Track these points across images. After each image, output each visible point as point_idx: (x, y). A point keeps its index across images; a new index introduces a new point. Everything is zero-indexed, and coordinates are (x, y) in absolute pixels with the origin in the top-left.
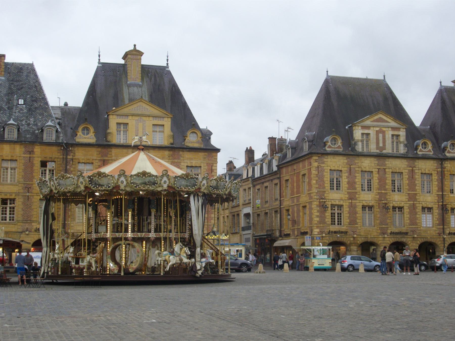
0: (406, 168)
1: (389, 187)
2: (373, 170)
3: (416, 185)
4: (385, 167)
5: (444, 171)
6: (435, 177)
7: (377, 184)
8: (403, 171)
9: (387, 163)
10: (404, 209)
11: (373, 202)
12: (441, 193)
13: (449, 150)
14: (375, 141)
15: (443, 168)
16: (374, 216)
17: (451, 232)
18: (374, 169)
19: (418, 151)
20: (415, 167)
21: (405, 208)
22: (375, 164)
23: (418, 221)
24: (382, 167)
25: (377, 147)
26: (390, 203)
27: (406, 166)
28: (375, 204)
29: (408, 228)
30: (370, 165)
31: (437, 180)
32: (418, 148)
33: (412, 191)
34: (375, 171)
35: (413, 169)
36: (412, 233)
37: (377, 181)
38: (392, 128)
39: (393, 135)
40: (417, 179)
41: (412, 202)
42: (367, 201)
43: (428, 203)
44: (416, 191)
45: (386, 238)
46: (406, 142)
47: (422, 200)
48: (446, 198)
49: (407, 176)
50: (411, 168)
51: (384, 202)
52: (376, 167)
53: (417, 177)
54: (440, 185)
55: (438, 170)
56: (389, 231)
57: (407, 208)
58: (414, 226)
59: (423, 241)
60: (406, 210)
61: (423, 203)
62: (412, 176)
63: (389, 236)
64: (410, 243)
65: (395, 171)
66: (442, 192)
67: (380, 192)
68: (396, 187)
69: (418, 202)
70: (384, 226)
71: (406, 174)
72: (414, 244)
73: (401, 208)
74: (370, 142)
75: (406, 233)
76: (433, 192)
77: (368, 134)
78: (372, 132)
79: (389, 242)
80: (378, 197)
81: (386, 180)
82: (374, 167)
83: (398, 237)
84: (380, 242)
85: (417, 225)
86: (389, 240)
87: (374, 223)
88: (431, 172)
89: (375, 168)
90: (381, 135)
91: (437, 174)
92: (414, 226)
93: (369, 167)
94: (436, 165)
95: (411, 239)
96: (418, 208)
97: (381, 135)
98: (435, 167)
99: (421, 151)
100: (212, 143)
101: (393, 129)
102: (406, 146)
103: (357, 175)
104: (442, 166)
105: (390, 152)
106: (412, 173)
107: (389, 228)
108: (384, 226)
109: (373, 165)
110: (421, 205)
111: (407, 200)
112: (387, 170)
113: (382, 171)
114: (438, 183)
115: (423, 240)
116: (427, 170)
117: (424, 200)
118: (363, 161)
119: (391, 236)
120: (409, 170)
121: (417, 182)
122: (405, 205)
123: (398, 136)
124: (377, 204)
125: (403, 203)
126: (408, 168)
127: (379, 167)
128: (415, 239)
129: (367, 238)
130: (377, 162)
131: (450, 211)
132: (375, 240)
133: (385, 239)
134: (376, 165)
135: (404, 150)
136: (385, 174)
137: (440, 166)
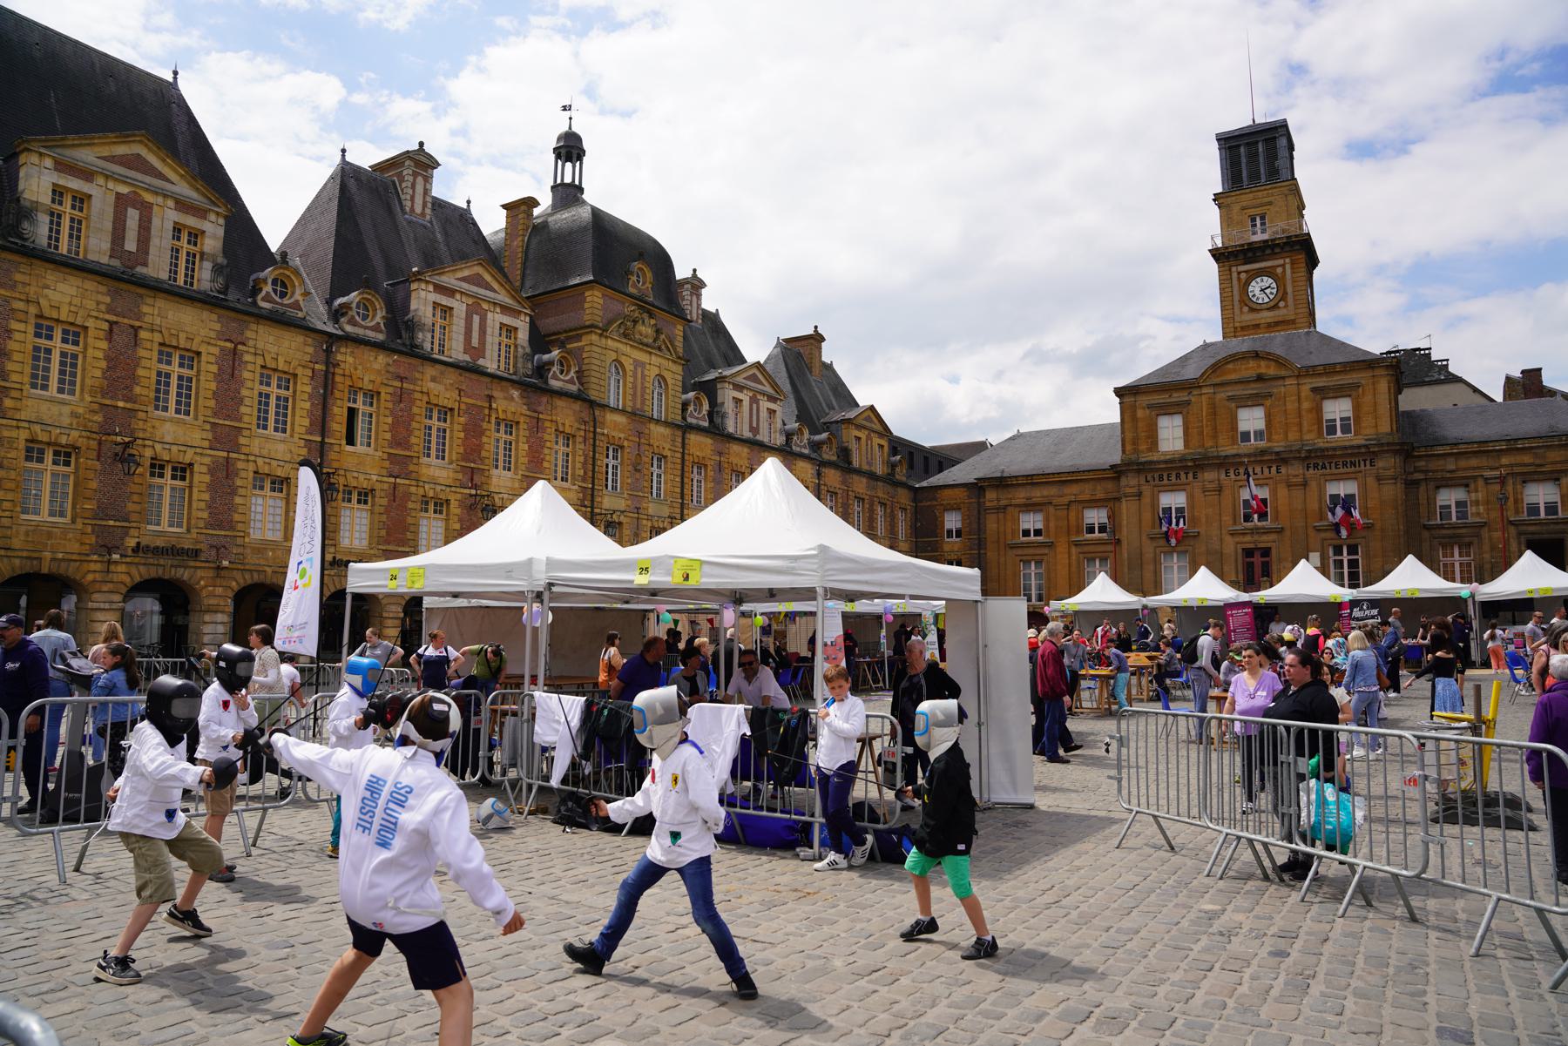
0: (212, 341)
1: (145, 392)
2: (90, 323)
3: (241, 401)
4: (137, 324)
5: (334, 374)
6: (305, 387)
7: (98, 373)
8: (203, 349)
9: (145, 309)
10: (192, 473)
11: (75, 434)
12: (319, 439)
13: (353, 317)
14: (109, 226)
15: (330, 364)
16: (76, 485)
17: (338, 557)
18: (91, 320)
19: (260, 297)
20: (244, 344)
21: (196, 468)
22: (98, 303)
23: (237, 517)
24: (126, 321)
25: (112, 249)
26: (144, 446)
27: (213, 334)
28: (82, 442)
29: (202, 538)
30: (76, 301)
31: (311, 396)
32: (261, 290)
33: (227, 417)
34: (96, 327)
35: (235, 348)
36: (213, 552)
37: (103, 364)
38: (177, 202)
39: (177, 230)
40: (249, 384)
41: (225, 454)
42: (49, 428)
43: (274, 463)
44: (240, 420)
45: (116, 562)
46: (221, 260)
47: (256, 451)
48: (332, 456)
49: (214, 368)
50: (228, 345)
51: (119, 439)
52: (101, 316)
53: (246, 375)
54: (320, 413)
55: (317, 366)
56: (131, 543)
57: (204, 469)
58: (223, 533)
59: (249, 582)
60: (201, 477)
61: (260, 461)
62: (230, 371)
63: (128, 560)
64: (206, 586)
65: (175, 344)
66: (323, 436)
67: (108, 402)
68: (173, 390)
69: (243, 457)
70: (111, 523)
71: (212, 359)
72: (219, 590)
73: (182, 471)
74: (88, 227)
75: (195, 554)
76: (293, 430)
77: (81, 200)
78: (101, 196)
79: (127, 580)
80: (98, 418)
81: (138, 365)
82: (94, 314)
83: (162, 562)
84: (90, 577)
85: (232, 528)
86: (129, 574)
87: (74, 507)
88: (295, 369)
89: (97, 318)
90: (133, 216)
91: (312, 378)
92: (223, 533)
93: (72, 308)
94: (310, 350)
95: (211, 573)
96: (243, 474)
97: (133, 216)
98: (308, 358)
99: (267, 298)
101: (182, 205)
102: (217, 269)
103: (21, 327)
104: (328, 357)
105: (164, 276)
106: (231, 363)
107: (133, 532)
108: (111, 523)
109: (91, 304)
110: (251, 467)
111: (206, 444)
112: (143, 334)
113: (124, 339)
114: (312, 404)
115: (249, 579)
116: (281, 360)
117: (265, 452)
118: (48, 282)
119: (137, 560)
120: (222, 349)
121: (245, 392)
122: (198, 458)
123: (195, 236)
124: (94, 444)
125: (190, 452)
126: (222, 343)
127: (114, 318)
128: (223, 573)
129: (35, 562)
130: (108, 300)
131: (340, 496)
132: (71, 571)
133: (112, 568)
134: (103, 307)
135: (213, 281)
136: (136, 345)
137: (322, 356)
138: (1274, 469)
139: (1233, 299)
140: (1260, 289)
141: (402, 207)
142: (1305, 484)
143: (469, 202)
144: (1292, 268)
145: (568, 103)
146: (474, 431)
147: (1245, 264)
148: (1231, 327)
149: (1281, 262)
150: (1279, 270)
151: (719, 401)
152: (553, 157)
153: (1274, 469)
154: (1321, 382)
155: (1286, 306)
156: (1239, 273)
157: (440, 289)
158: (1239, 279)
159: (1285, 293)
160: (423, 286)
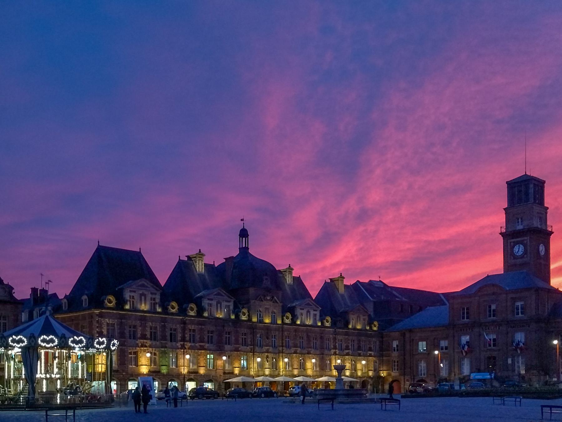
100: (19, 299)
138: (498, 328)
139: (508, 254)
140: (519, 250)
141: (196, 271)
142: (507, 333)
143: (214, 262)
144: (530, 240)
145: (242, 218)
146: (220, 335)
147: (513, 238)
148: (508, 266)
149: (526, 238)
150: (525, 242)
151: (296, 314)
152: (239, 237)
153: (498, 328)
154: (514, 296)
155: (527, 257)
156: (511, 243)
157: (209, 299)
158: (510, 245)
159: (527, 250)
160: (205, 299)
